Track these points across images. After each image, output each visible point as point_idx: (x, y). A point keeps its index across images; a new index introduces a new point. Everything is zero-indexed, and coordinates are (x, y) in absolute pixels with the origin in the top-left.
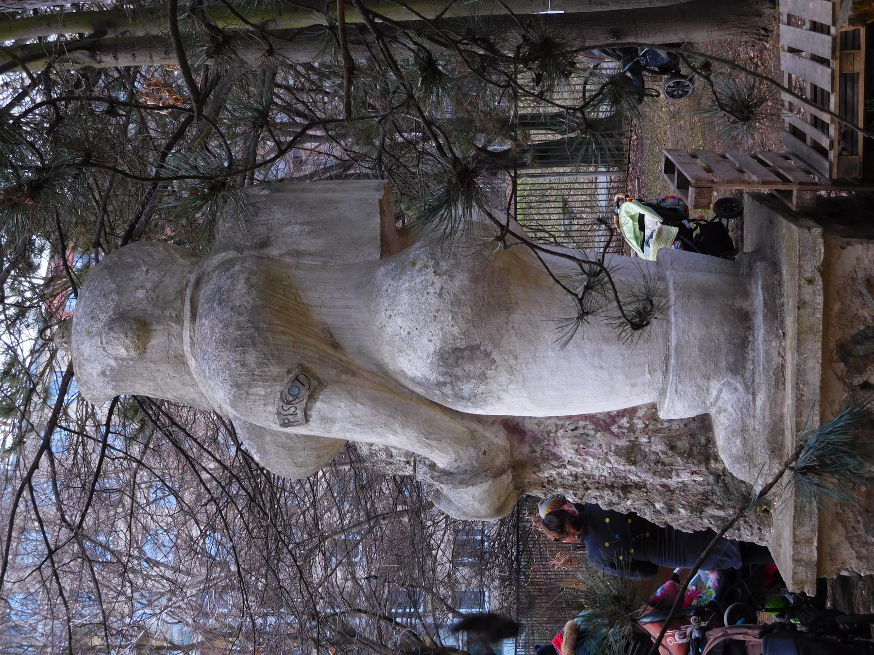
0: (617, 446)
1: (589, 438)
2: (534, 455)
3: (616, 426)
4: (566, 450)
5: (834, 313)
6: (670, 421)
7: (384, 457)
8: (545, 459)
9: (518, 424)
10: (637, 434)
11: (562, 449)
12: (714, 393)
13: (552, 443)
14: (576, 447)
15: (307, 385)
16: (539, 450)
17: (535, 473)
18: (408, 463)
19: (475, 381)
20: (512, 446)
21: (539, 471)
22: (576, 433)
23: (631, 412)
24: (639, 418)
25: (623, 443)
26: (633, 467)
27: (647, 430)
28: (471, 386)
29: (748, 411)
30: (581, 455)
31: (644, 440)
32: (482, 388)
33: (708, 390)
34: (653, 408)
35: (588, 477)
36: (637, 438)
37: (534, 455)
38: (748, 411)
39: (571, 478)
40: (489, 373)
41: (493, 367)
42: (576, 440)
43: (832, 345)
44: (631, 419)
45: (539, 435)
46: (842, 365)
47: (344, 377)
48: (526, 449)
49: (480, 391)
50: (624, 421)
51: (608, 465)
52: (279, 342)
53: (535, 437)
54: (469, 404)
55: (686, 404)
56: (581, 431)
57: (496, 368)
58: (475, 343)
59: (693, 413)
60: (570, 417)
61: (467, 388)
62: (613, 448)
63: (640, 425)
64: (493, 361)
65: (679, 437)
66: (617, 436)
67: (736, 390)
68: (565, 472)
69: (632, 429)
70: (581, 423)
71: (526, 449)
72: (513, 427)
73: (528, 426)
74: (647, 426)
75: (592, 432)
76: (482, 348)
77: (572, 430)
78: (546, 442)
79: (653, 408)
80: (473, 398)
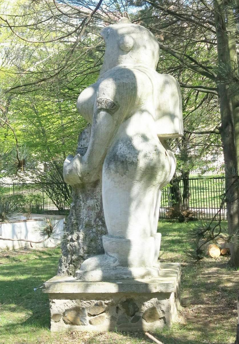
0: (91, 221)
1: (94, 211)
2: (87, 191)
3: (99, 220)
4: (91, 202)
5: (144, 297)
6: (102, 240)
7: (83, 137)
8: (86, 195)
9: (98, 185)
10: (96, 228)
11: (90, 201)
12: (113, 255)
13: (92, 197)
14: (91, 206)
15: (112, 109)
16: (89, 193)
17: (81, 191)
18: (82, 146)
19: (115, 169)
20: (90, 183)
21: (81, 193)
22: (96, 205)
23: (104, 224)
24: (102, 228)
25: (93, 223)
26: (84, 227)
27: (97, 231)
28: (113, 168)
29: (107, 267)
30: (88, 208)
31: (94, 230)
32: (112, 172)
33: (114, 253)
34: (106, 233)
35: (80, 211)
36: (95, 228)
37: (87, 191)
38: (107, 267)
39: (79, 204)
40: (118, 174)
41: (120, 176)
42: (93, 206)
43: (132, 296)
44: (101, 225)
45: (94, 193)
46: (125, 300)
47: (115, 122)
48: (89, 188)
49: (111, 171)
50: (100, 223)
51: (85, 218)
52: (127, 98)
53: (93, 191)
54: (107, 167)
55: (108, 245)
56: (96, 208)
57: (120, 177)
58: (129, 169)
59: (105, 247)
60: (102, 203)
61: (112, 166)
62: (91, 219)
63: (99, 229)
64: (122, 176)
65: (95, 243)
66: (95, 221)
67: (114, 263)
68: (81, 202)
69: (97, 226)
70: (99, 208)
71: (89, 188)
72: (97, 183)
73: (98, 189)
74: (99, 231)
75: (96, 212)
76: (127, 172)
77: (97, 205)
78: (92, 195)
79: (106, 233)
80: (109, 168)
